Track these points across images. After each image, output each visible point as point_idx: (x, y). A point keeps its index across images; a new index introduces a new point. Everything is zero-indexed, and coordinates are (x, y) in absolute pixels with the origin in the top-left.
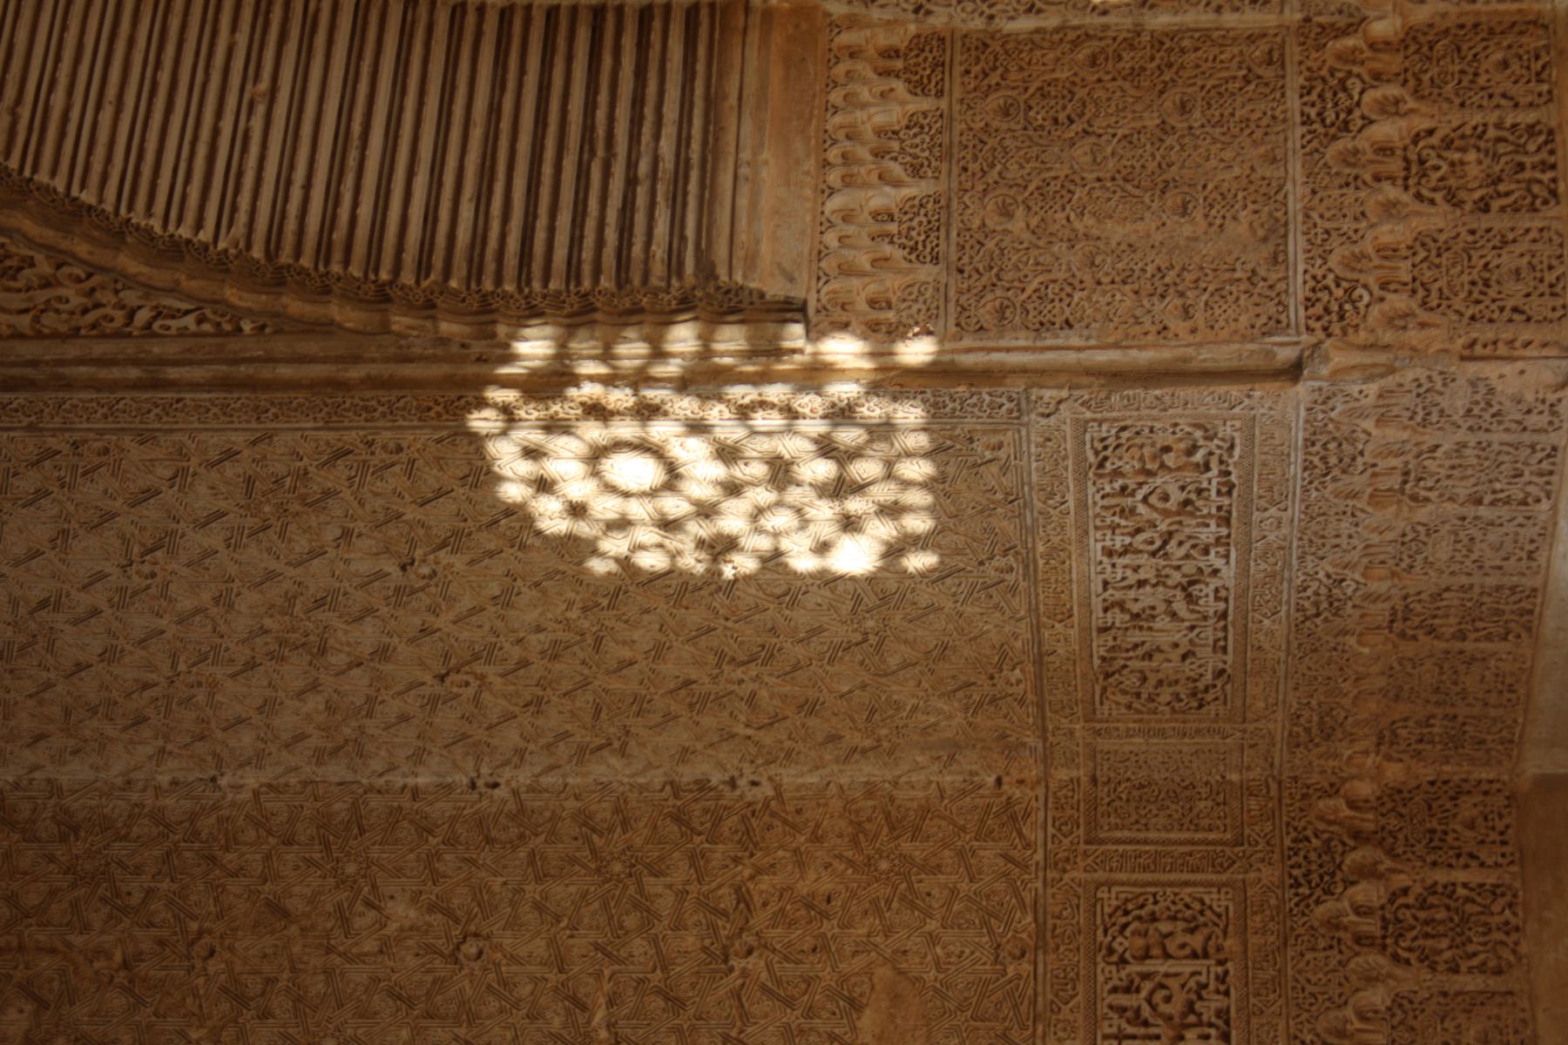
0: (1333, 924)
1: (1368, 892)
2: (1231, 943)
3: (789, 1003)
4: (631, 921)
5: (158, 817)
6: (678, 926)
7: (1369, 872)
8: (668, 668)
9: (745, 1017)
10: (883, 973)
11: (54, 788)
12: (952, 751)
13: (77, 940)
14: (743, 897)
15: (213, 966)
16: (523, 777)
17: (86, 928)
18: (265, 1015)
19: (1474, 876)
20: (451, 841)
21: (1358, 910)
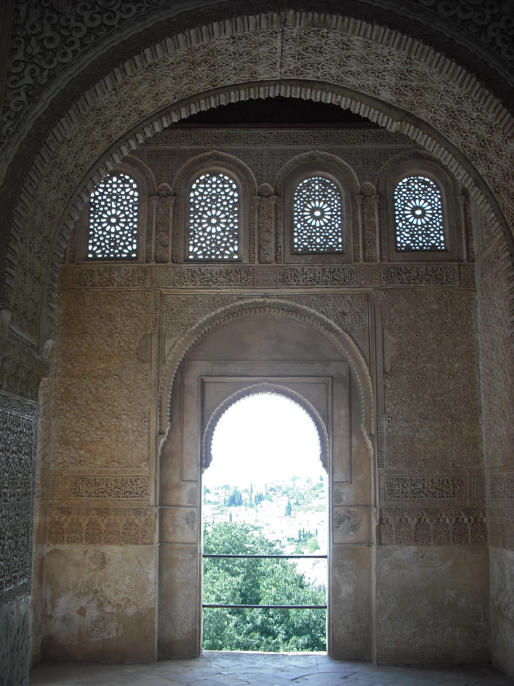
0: (460, 514)
1: (466, 520)
2: (456, 498)
3: (443, 428)
4: (456, 402)
5: (472, 324)
6: (456, 410)
7: (469, 520)
8: (493, 406)
9: (440, 421)
10: (449, 443)
11: (476, 307)
12: (487, 453)
13: (449, 314)
14: (461, 420)
15: (446, 336)
16: (481, 383)
17: (451, 315)
18: (438, 346)
19: (470, 537)
20: (469, 372)
21: (463, 519)
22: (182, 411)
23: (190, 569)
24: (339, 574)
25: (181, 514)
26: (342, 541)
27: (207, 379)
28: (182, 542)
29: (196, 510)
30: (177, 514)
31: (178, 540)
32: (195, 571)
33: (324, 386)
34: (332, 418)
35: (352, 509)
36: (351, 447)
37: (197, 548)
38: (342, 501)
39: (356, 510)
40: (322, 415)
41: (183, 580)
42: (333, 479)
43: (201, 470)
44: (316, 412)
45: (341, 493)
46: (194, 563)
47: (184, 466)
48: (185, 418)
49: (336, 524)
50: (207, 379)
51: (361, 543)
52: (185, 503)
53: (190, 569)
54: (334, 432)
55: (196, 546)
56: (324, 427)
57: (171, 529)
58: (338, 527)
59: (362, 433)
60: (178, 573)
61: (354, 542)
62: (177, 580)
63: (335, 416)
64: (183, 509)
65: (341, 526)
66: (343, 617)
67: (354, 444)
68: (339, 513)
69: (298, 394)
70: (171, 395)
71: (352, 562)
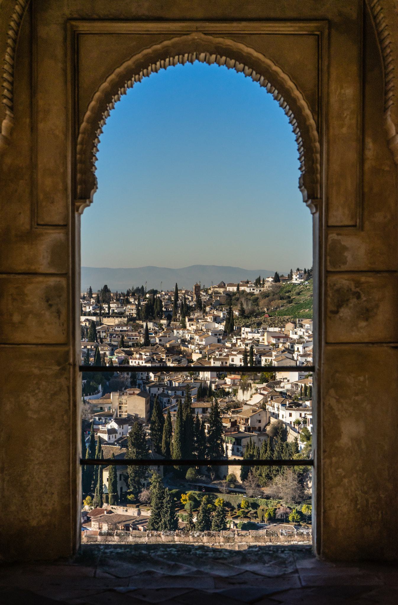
22: (33, 90)
23: (55, 394)
24: (338, 401)
25: (35, 291)
26: (343, 338)
27: (84, 27)
28: (40, 341)
29: (63, 281)
30: (28, 289)
31: (31, 339)
32: (63, 397)
33: (311, 41)
34: (328, 102)
35: (363, 279)
36: (362, 160)
37: (67, 353)
38: (345, 263)
39: (371, 280)
40: (307, 98)
41: (43, 413)
42: (327, 222)
43: (73, 204)
44: (297, 93)
45: (345, 248)
46: (63, 381)
47: (41, 196)
48: (41, 103)
49: (331, 307)
50: (84, 27)
51: (380, 343)
52: (43, 268)
53: (55, 394)
54: (331, 131)
55: (66, 349)
56: (312, 122)
57: (16, 318)
58: (337, 312)
59: (386, 132)
60: (32, 400)
61: (366, 340)
62: (30, 414)
63: (334, 100)
64: (40, 279)
65: (342, 310)
66: (346, 481)
67: (369, 154)
68: (338, 286)
69: (260, 56)
70: (12, 58)
71: (362, 379)
